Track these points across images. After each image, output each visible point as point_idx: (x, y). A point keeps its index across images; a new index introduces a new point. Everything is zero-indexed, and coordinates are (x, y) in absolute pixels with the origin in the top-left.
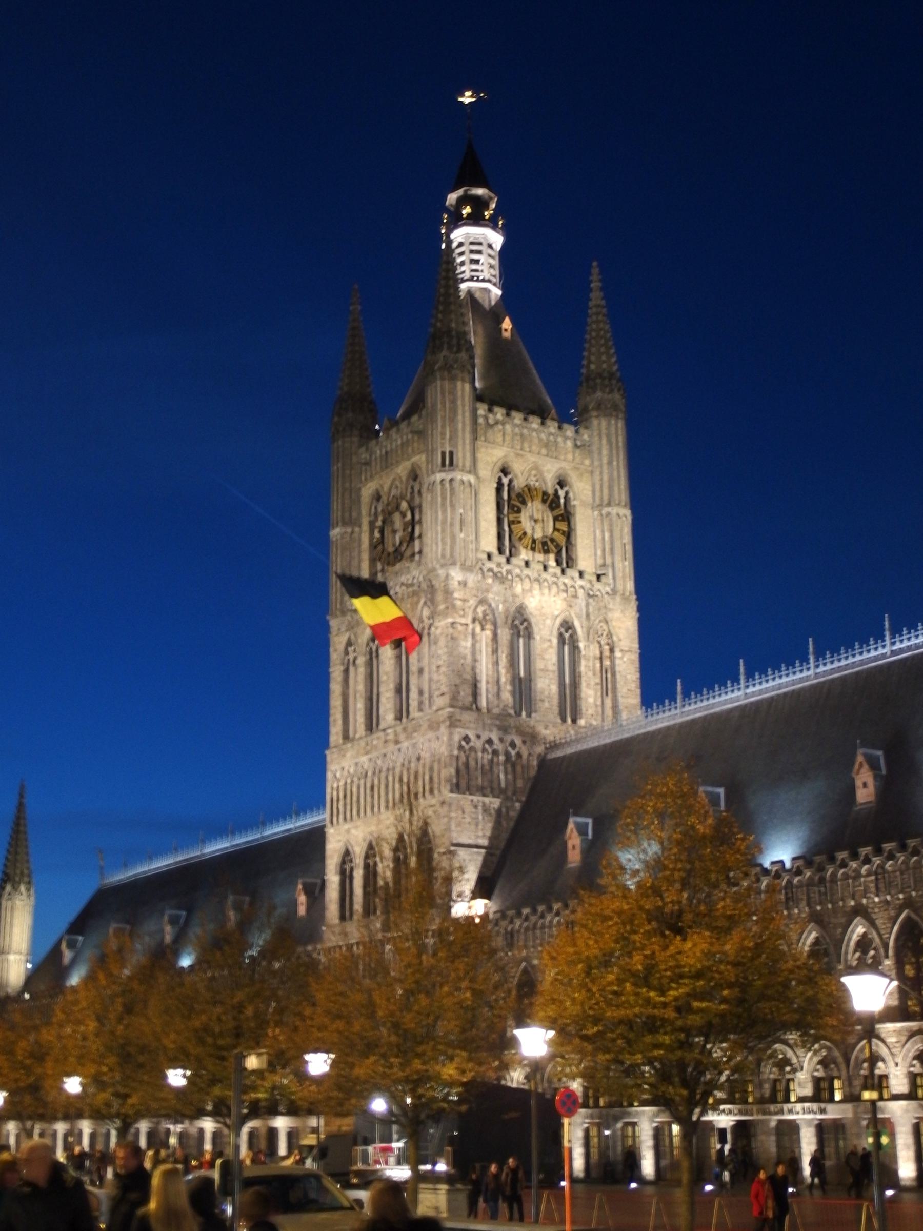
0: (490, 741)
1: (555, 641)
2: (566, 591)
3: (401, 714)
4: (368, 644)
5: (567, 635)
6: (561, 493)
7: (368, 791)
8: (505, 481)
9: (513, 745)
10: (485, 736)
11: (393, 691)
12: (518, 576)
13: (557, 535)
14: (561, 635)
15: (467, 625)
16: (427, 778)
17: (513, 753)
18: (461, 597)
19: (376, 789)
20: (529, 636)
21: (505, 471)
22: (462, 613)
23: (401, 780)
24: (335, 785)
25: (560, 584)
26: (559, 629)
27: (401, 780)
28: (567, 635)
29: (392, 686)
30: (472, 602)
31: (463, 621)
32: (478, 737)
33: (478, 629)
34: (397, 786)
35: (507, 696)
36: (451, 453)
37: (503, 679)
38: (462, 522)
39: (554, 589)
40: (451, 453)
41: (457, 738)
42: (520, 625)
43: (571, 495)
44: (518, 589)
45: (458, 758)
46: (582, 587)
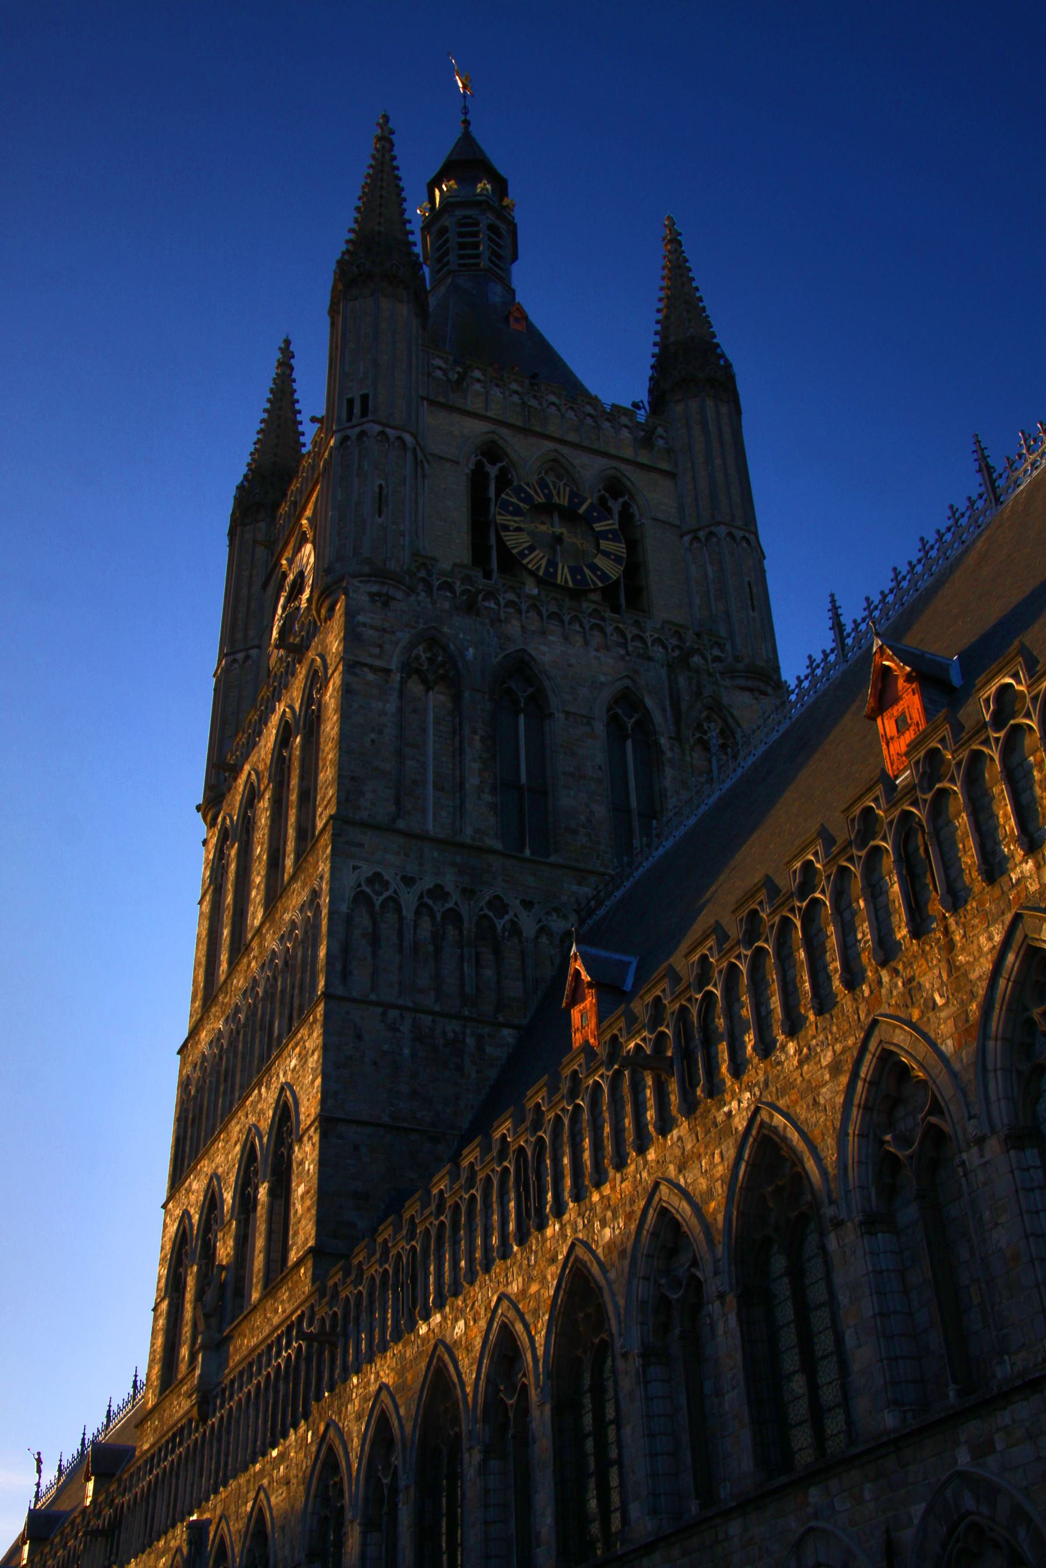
0: (438, 892)
1: (600, 728)
2: (624, 645)
5: (630, 723)
6: (616, 506)
8: (493, 471)
9: (499, 905)
10: (427, 883)
12: (510, 603)
13: (600, 561)
14: (614, 722)
15: (387, 671)
17: (499, 924)
20: (539, 708)
21: (491, 452)
22: (377, 651)
25: (609, 629)
26: (609, 710)
28: (630, 723)
30: (404, 637)
31: (379, 663)
32: (408, 881)
33: (415, 687)
36: (365, 398)
37: (473, 781)
38: (381, 500)
39: (596, 639)
40: (365, 398)
41: (350, 880)
42: (519, 687)
43: (634, 509)
44: (514, 627)
45: (349, 919)
46: (658, 641)
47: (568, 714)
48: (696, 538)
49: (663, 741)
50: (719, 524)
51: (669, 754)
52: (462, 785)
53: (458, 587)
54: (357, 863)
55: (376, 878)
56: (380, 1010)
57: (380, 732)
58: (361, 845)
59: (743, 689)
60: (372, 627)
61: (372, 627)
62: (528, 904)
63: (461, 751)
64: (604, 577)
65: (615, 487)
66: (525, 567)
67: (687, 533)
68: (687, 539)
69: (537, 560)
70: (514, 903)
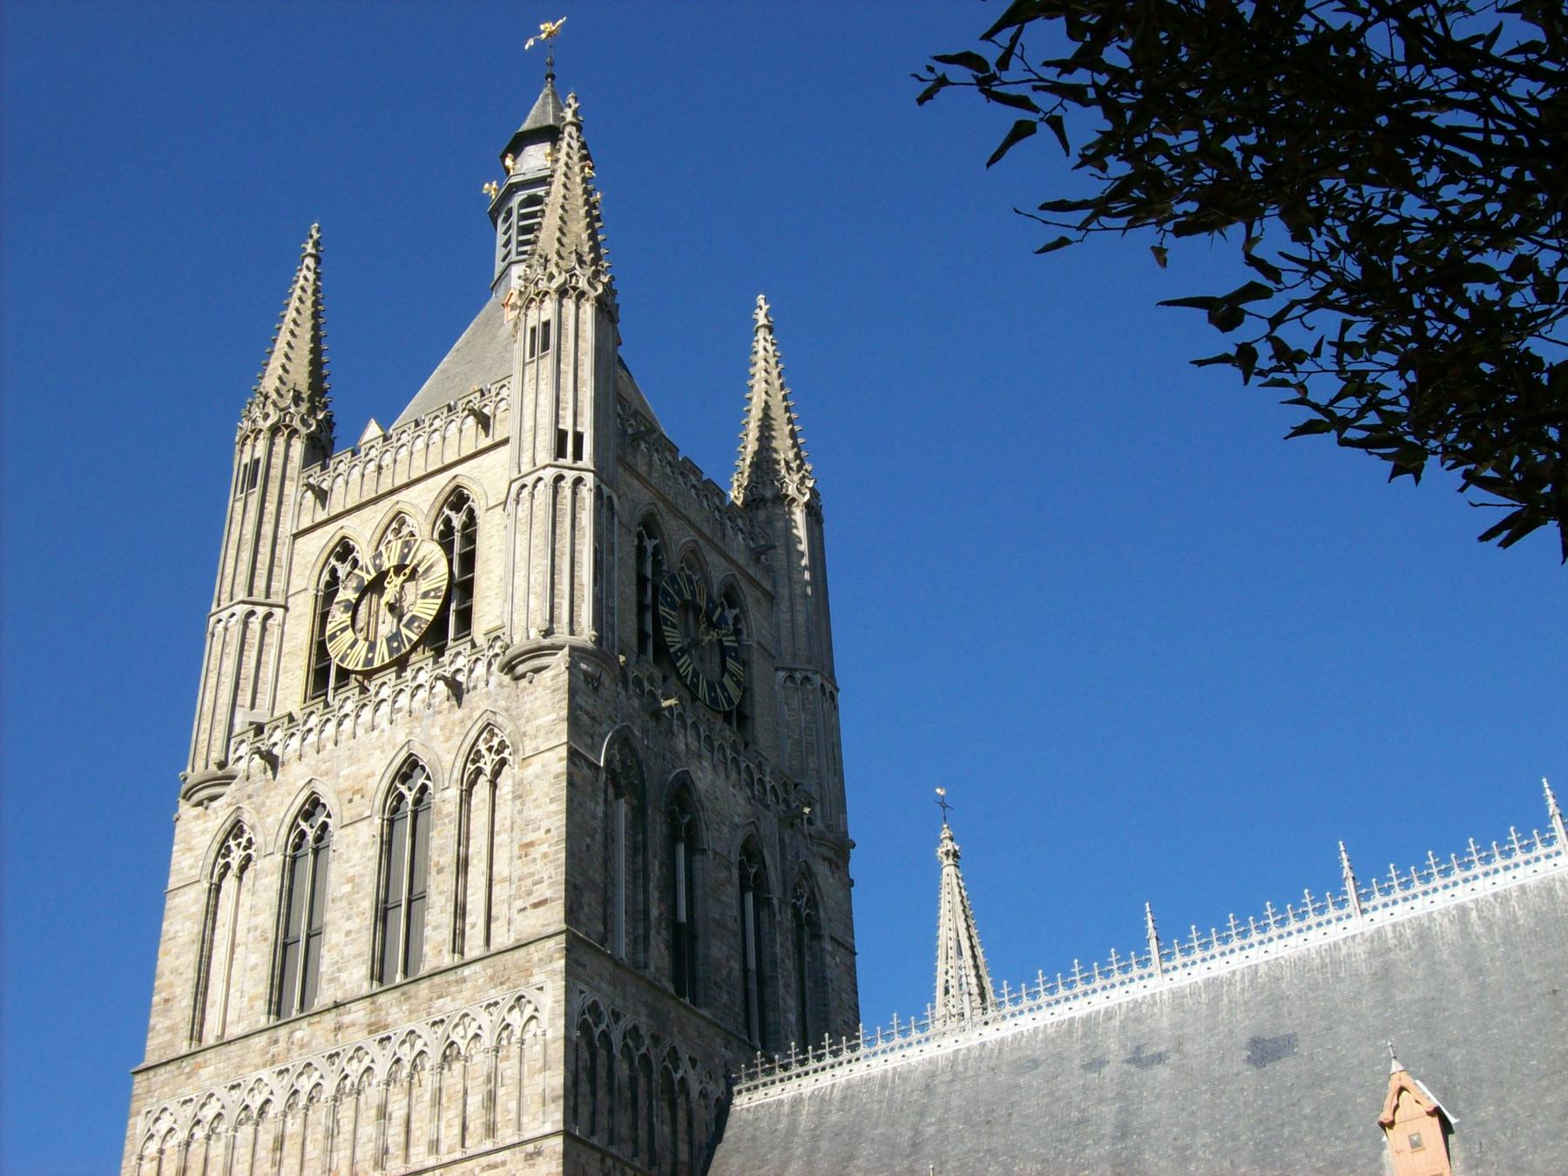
3: (393, 960)
4: (294, 825)
7: (264, 1153)
8: (649, 544)
9: (674, 1055)
10: (627, 1022)
11: (370, 915)
16: (475, 1100)
18: (590, 709)
19: (291, 1147)
23: (383, 1113)
24: (152, 1148)
27: (383, 1113)
29: (367, 905)
32: (616, 1016)
34: (368, 1130)
35: (659, 955)
37: (654, 913)
41: (578, 1001)
42: (681, 813)
47: (715, 853)
48: (791, 678)
49: (775, 902)
50: (816, 673)
51: (778, 918)
52: (646, 913)
53: (647, 686)
54: (584, 988)
55: (594, 1008)
56: (598, 1156)
57: (593, 838)
58: (584, 967)
59: (825, 859)
60: (587, 713)
61: (587, 713)
62: (693, 1062)
63: (646, 877)
64: (729, 700)
65: (731, 596)
66: (677, 670)
67: (783, 669)
68: (782, 674)
69: (685, 664)
70: (685, 1058)
